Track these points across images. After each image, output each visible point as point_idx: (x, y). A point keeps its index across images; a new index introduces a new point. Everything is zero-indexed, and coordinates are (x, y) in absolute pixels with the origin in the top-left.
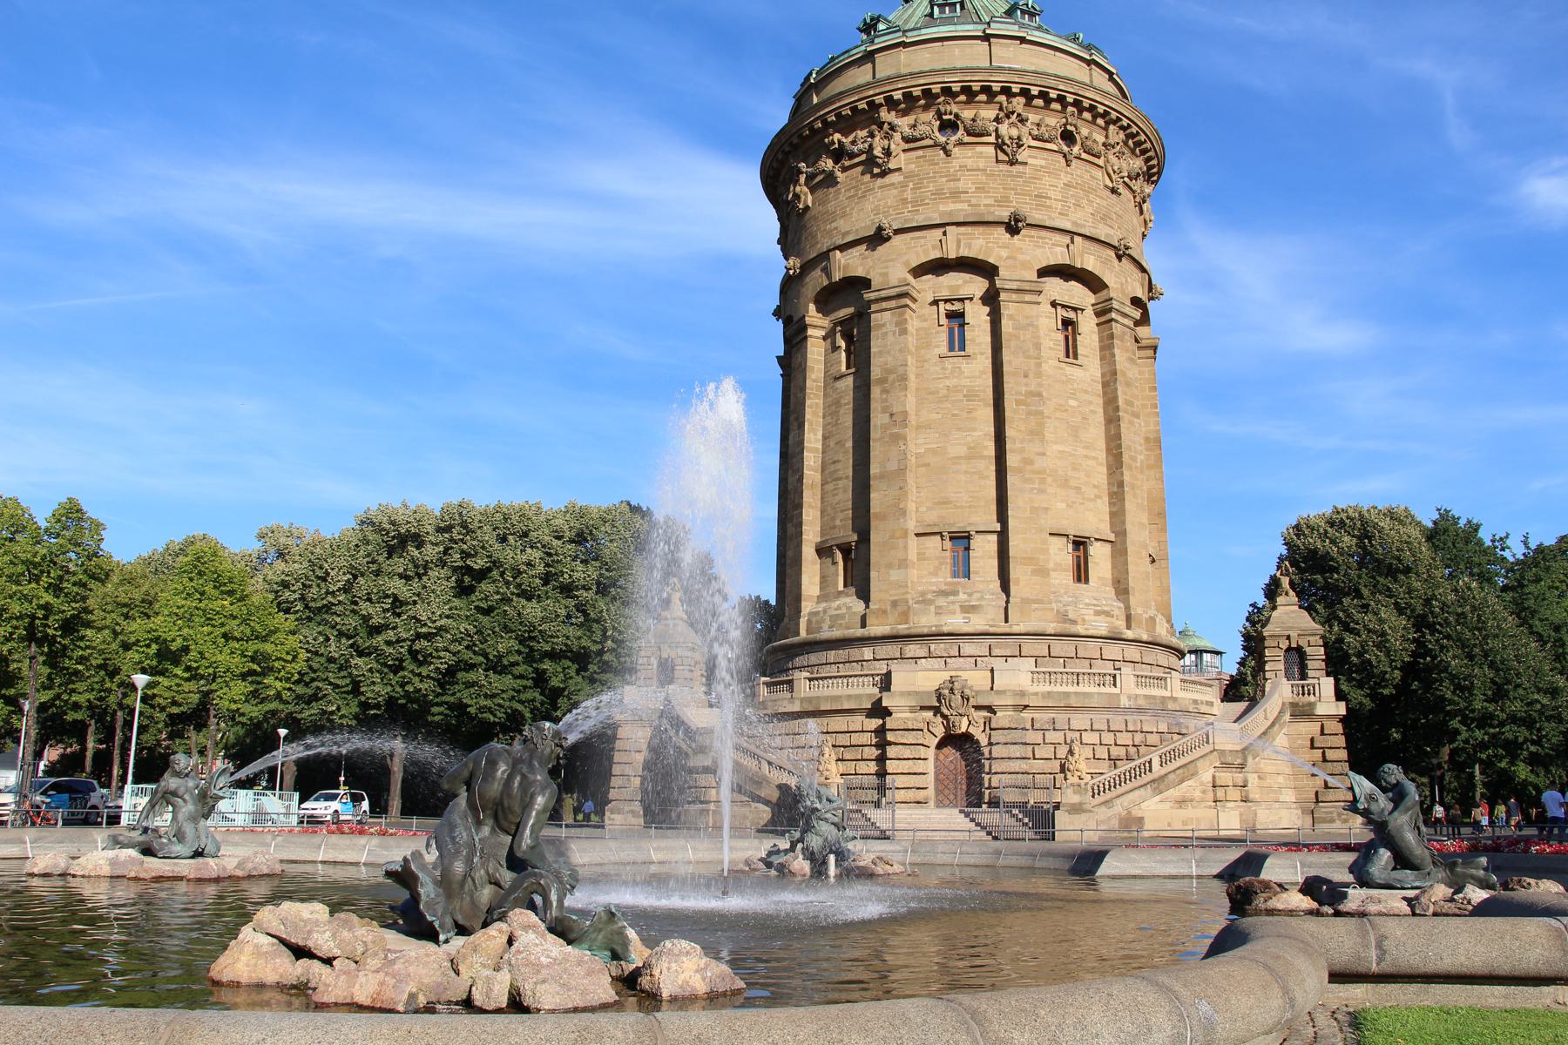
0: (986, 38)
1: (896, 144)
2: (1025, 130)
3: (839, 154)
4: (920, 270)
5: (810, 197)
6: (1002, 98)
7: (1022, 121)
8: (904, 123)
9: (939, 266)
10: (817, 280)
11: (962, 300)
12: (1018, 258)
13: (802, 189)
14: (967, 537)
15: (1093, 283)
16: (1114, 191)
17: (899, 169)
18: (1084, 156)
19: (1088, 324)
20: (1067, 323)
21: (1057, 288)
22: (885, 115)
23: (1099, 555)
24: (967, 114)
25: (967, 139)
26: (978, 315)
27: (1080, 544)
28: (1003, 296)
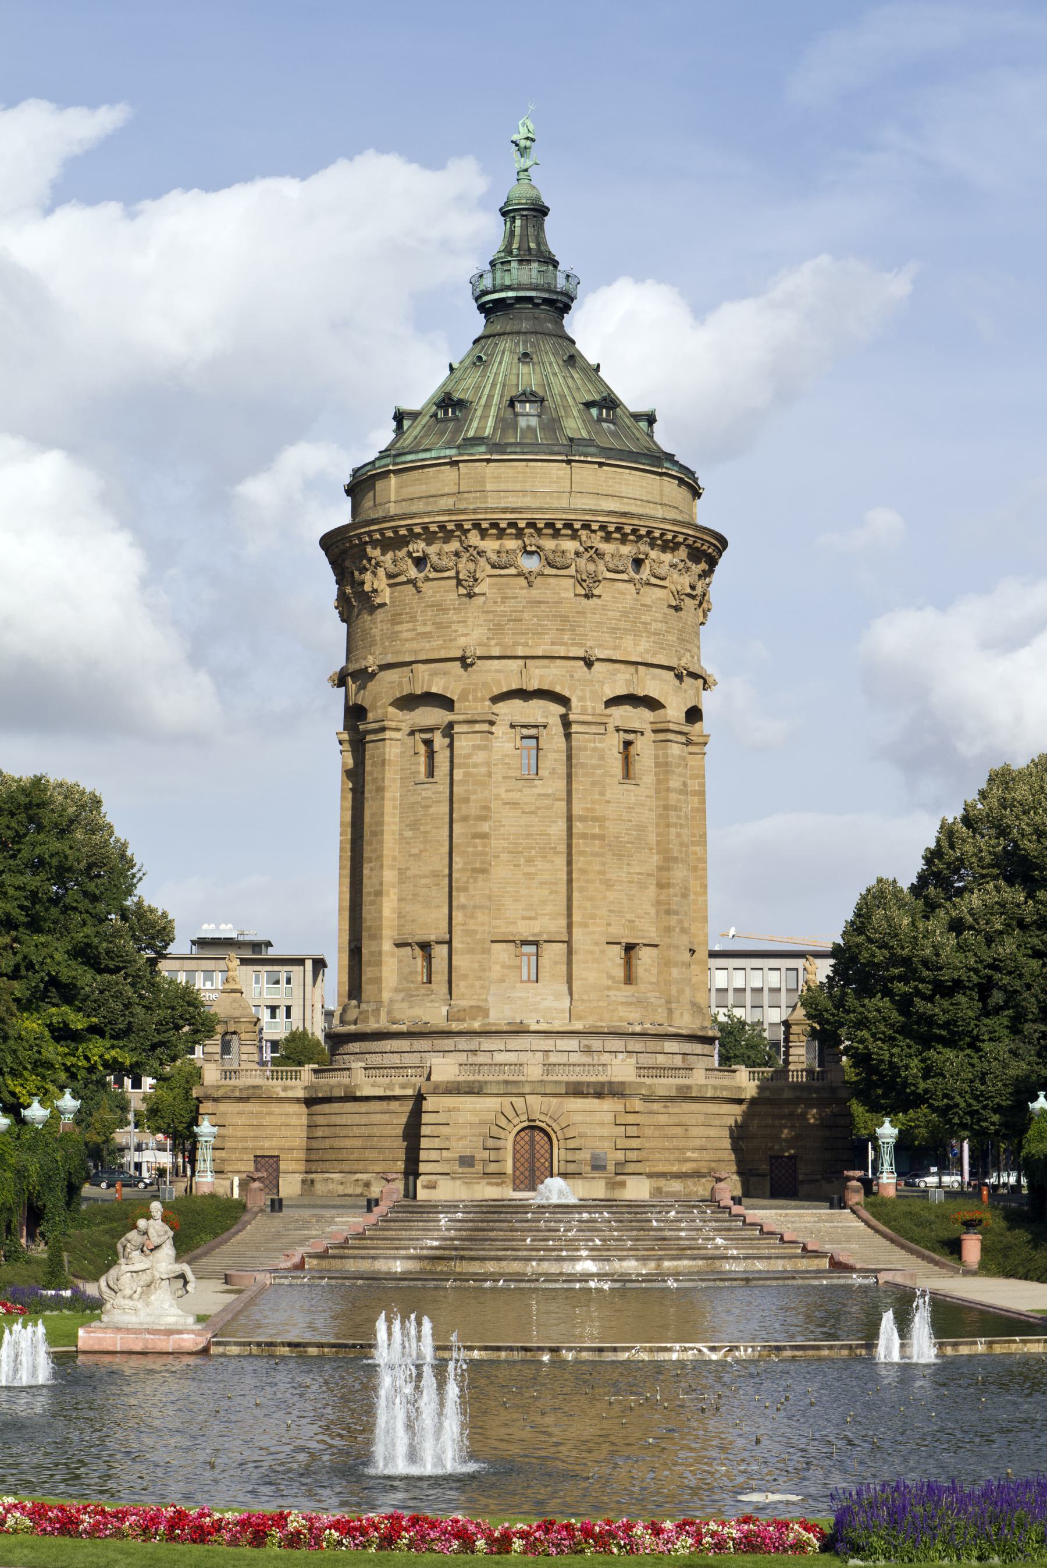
0: (569, 462)
1: (484, 568)
2: (601, 564)
3: (420, 562)
5: (388, 590)
6: (583, 533)
7: (600, 555)
11: (537, 726)
12: (588, 691)
14: (536, 943)
15: (652, 704)
16: (677, 609)
17: (484, 594)
18: (654, 581)
19: (644, 746)
20: (627, 744)
22: (474, 538)
23: (645, 957)
24: (549, 544)
25: (549, 571)
28: (575, 728)
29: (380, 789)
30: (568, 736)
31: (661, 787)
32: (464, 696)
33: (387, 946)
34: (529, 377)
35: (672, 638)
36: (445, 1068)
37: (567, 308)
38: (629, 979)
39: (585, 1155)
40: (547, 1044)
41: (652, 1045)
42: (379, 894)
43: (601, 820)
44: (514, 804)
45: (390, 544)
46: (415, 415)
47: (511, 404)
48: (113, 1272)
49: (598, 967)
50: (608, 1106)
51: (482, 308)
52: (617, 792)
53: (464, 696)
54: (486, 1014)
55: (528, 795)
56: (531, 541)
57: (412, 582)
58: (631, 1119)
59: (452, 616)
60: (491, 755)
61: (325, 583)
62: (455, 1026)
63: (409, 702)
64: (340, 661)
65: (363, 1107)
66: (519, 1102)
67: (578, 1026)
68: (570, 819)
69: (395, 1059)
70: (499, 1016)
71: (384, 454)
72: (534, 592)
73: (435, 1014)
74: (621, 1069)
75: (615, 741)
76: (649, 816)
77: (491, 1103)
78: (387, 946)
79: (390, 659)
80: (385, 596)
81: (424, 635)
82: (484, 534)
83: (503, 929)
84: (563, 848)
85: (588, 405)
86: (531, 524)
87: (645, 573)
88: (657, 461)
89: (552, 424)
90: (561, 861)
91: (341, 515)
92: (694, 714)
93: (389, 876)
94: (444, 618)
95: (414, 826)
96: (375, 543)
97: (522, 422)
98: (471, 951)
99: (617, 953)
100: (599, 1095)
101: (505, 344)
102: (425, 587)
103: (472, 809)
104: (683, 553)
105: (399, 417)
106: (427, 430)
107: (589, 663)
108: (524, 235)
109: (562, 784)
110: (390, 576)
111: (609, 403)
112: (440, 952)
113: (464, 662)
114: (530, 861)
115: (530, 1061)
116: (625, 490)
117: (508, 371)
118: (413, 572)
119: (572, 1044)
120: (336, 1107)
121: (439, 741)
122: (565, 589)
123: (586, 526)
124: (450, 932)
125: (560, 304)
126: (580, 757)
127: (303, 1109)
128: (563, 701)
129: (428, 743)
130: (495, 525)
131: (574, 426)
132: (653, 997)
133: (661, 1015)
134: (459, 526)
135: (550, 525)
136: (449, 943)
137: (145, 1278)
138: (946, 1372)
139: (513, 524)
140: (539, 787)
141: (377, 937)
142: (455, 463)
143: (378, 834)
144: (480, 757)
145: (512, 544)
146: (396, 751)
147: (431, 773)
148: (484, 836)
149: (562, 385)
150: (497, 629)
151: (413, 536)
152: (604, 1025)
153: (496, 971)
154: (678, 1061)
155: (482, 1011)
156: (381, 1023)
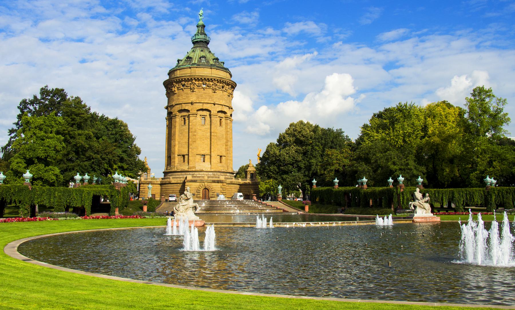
1: (196, 87)
3: (183, 85)
4: (198, 110)
7: (217, 85)
8: (197, 83)
9: (202, 110)
10: (178, 108)
12: (214, 110)
13: (176, 89)
15: (225, 113)
19: (223, 120)
21: (221, 115)
22: (194, 81)
23: (223, 158)
24: (208, 83)
26: (208, 118)
27: (221, 156)
29: (175, 127)
30: (210, 117)
31: (226, 128)
32: (192, 110)
33: (176, 155)
34: (203, 54)
35: (228, 101)
36: (189, 177)
37: (208, 44)
38: (221, 162)
39: (215, 194)
40: (207, 173)
41: (225, 174)
42: (175, 146)
43: (216, 133)
44: (200, 130)
45: (177, 82)
46: (181, 60)
47: (200, 58)
48: (177, 206)
49: (215, 159)
50: (220, 185)
51: (194, 43)
52: (219, 128)
53: (192, 110)
54: (195, 168)
55: (203, 128)
56: (205, 82)
57: (182, 89)
58: (224, 187)
59: (190, 95)
60: (196, 121)
61: (164, 90)
62: (190, 170)
63: (181, 111)
64: (166, 105)
65: (172, 185)
66: (203, 184)
67: (212, 170)
68: (211, 133)
69: (178, 176)
70: (198, 168)
71: (176, 66)
72: (205, 91)
73: (186, 168)
74: (222, 178)
75: (218, 119)
76: (224, 133)
77: (198, 184)
78: (176, 155)
79: (178, 103)
80: (177, 92)
81: (185, 99)
82: (196, 80)
83: (198, 153)
84: (209, 138)
85: (214, 59)
86: (205, 79)
87: (224, 89)
88: (226, 70)
89: (208, 62)
90: (209, 140)
91: (167, 78)
92: (231, 115)
93: (177, 143)
94: (188, 96)
95: (181, 134)
96: (175, 82)
97: (202, 61)
98: (192, 156)
99: (219, 157)
100: (218, 182)
101: (198, 48)
102: (184, 90)
103: (193, 130)
104: (230, 86)
105: (178, 61)
106: (184, 62)
107: (214, 104)
108: (201, 30)
109: (209, 126)
110: (178, 88)
111: (217, 59)
112: (186, 157)
113: (192, 103)
114: (203, 140)
115: (205, 176)
116: (221, 74)
117: (198, 53)
118: (182, 87)
119: (211, 173)
120: (167, 185)
121: (186, 118)
122: (210, 91)
123: (215, 80)
124: (188, 153)
125: (207, 43)
126: (213, 121)
127: (159, 186)
128: (210, 111)
129: (184, 119)
130: (198, 79)
131: (212, 62)
132: (225, 165)
133: (226, 169)
134: (191, 79)
135: (208, 79)
136: (188, 155)
137: (186, 207)
138: (395, 227)
139: (201, 79)
140: (205, 127)
141: (174, 154)
142: (190, 68)
143: (175, 135)
144: (194, 121)
145: (201, 82)
146: (178, 120)
147: (185, 123)
148: (195, 135)
149: (208, 55)
150: (198, 98)
151: (182, 81)
152: (217, 170)
153: (197, 160)
154: (229, 177)
155: (195, 167)
156: (175, 170)
